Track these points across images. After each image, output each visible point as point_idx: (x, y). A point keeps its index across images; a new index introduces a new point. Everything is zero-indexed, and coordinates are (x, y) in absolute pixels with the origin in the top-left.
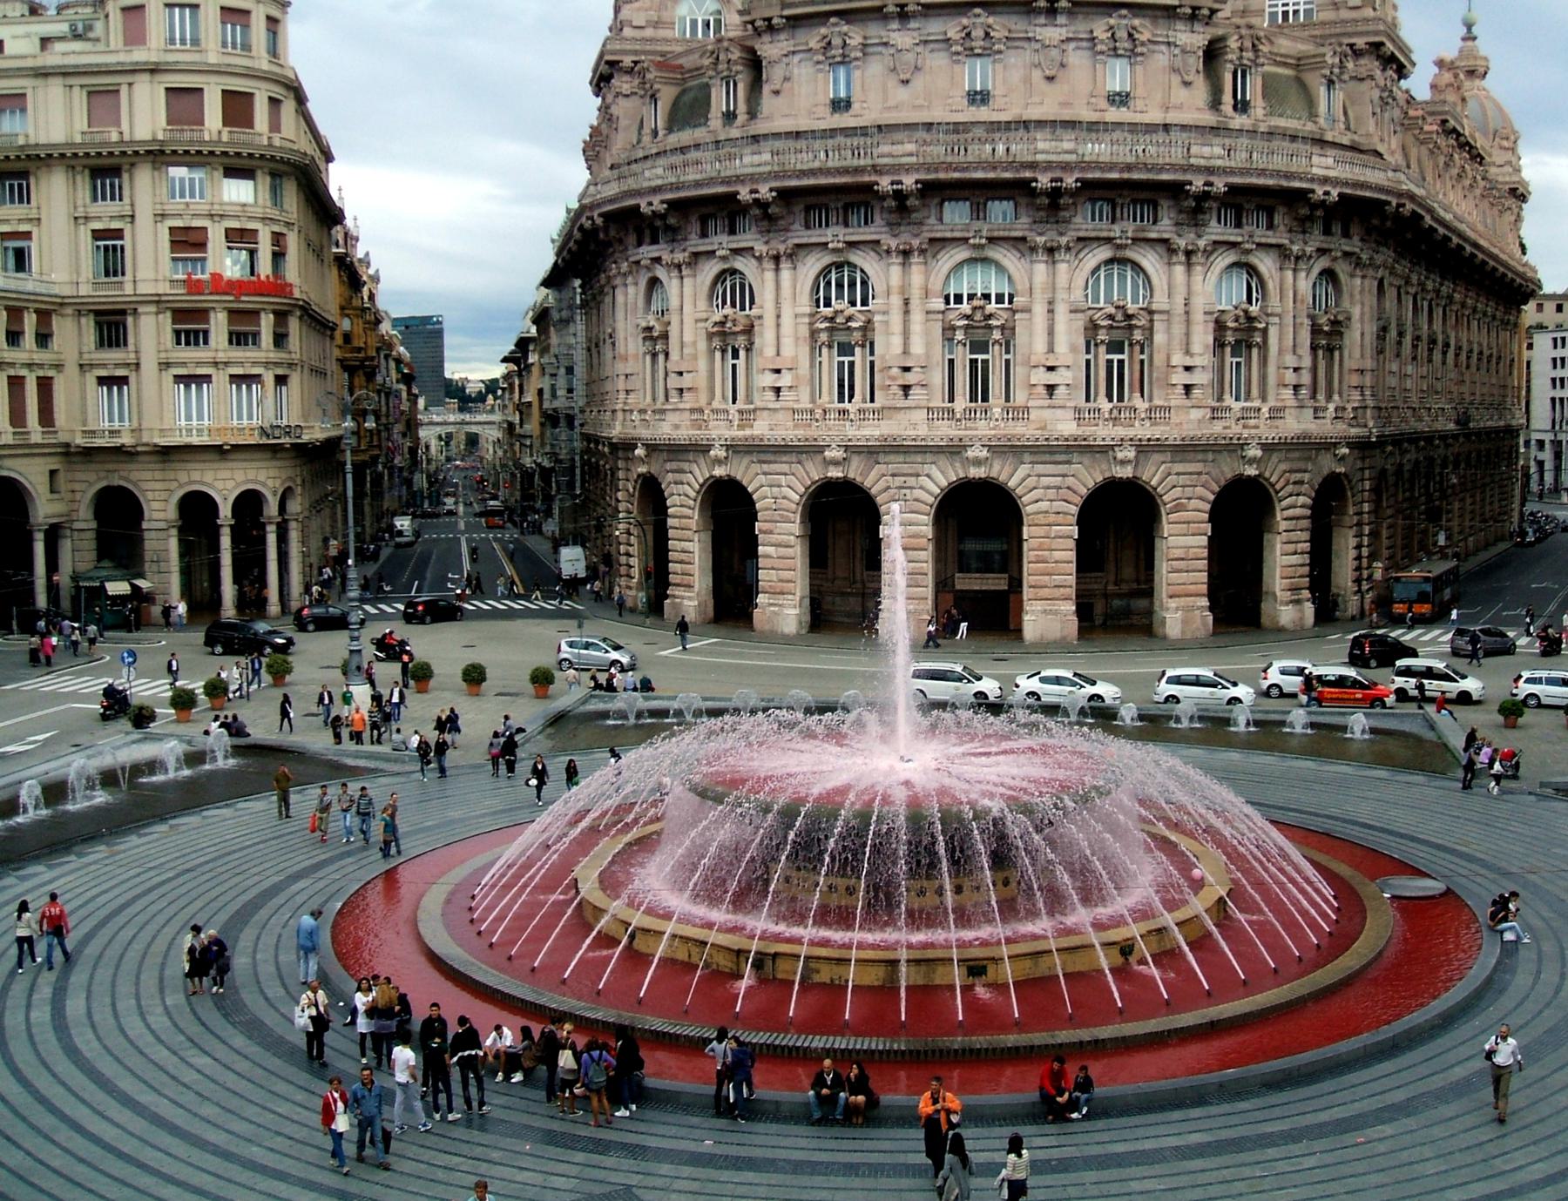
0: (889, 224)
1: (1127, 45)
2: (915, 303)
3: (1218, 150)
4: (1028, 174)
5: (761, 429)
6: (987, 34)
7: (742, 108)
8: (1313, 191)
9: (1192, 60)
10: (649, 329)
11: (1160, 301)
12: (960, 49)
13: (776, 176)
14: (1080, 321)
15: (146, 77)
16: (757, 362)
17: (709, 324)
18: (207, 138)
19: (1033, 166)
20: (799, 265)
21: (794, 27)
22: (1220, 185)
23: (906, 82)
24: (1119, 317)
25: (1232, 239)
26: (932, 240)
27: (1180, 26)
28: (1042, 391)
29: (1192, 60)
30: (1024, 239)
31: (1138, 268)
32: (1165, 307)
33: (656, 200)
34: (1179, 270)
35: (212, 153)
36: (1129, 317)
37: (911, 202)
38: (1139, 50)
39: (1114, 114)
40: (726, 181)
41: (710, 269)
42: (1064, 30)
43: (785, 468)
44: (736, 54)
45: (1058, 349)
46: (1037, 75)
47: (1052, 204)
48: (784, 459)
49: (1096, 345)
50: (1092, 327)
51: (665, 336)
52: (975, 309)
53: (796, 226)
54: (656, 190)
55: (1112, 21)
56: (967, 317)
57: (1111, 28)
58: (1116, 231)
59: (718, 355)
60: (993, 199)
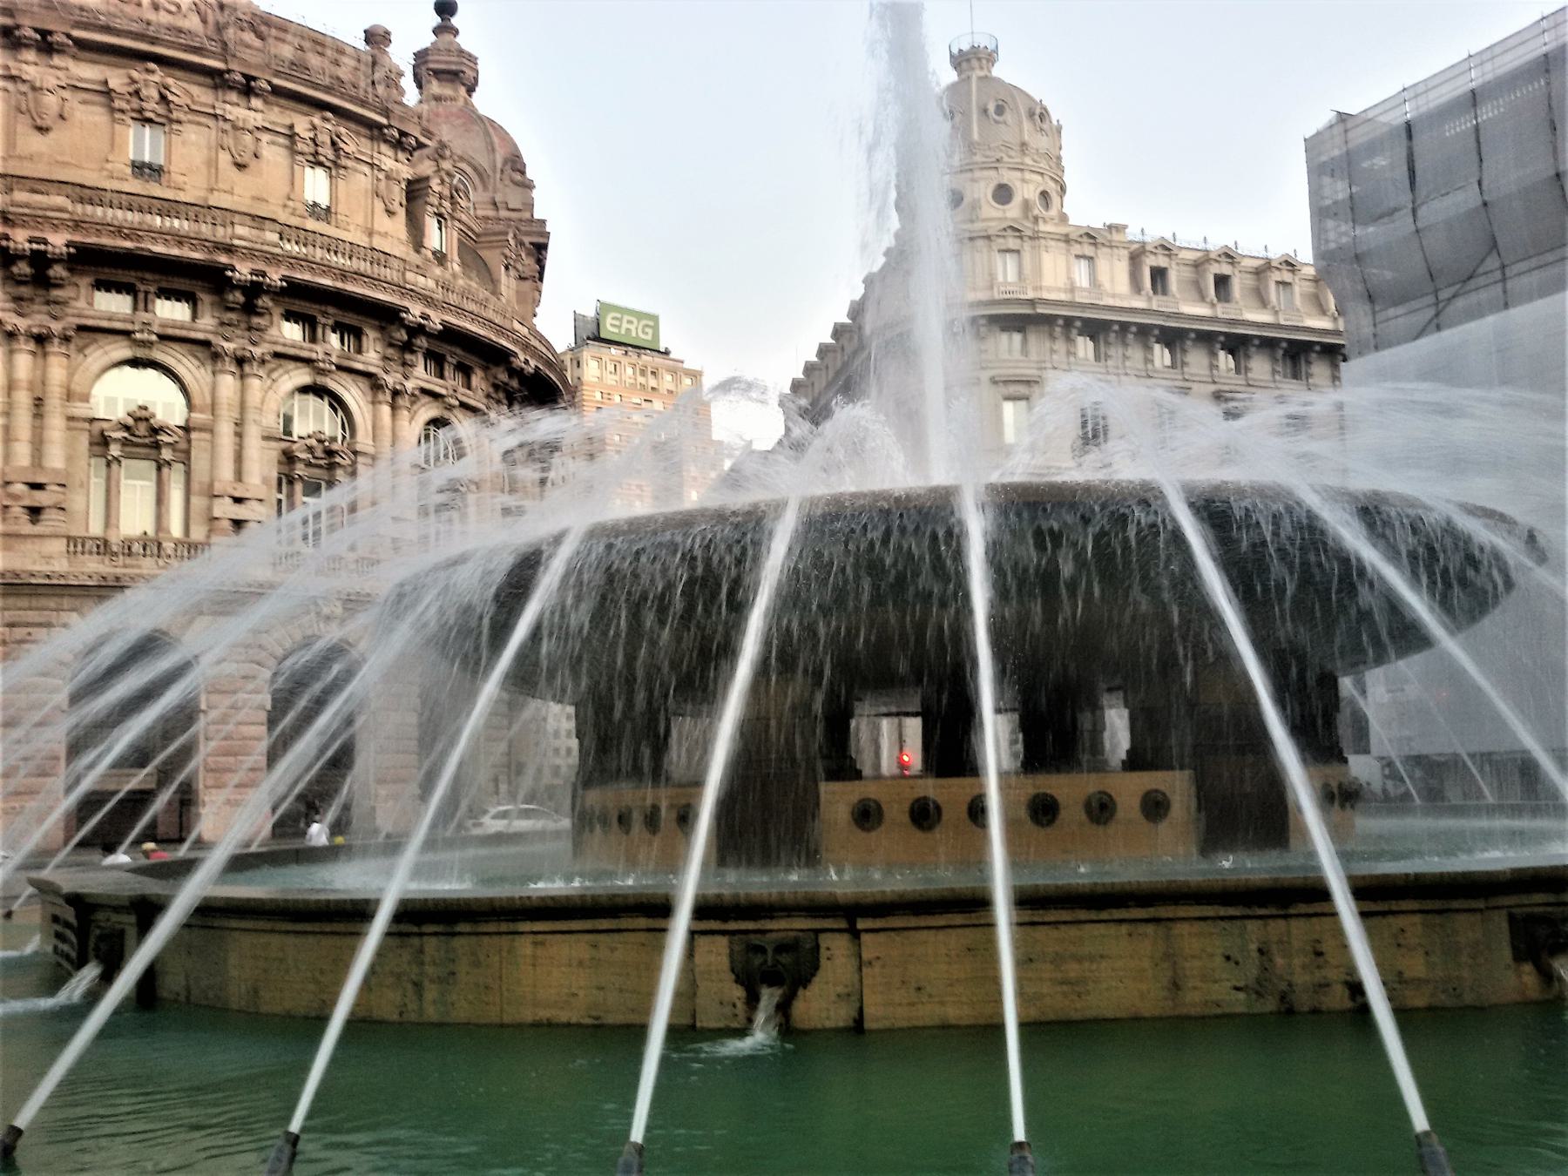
0: (18, 299)
1: (330, 153)
2: (54, 402)
3: (431, 284)
4: (223, 259)
6: (163, 98)
8: (515, 355)
9: (396, 189)
11: (364, 441)
12: (124, 106)
14: (274, 451)
19: (229, 249)
22: (436, 320)
23: (42, 130)
24: (319, 453)
25: (438, 389)
26: (81, 329)
27: (384, 148)
28: (226, 524)
29: (396, 189)
30: (206, 344)
31: (337, 403)
32: (371, 450)
34: (386, 410)
36: (330, 453)
37: (58, 271)
38: (344, 162)
39: (311, 224)
42: (259, 116)
45: (245, 478)
46: (224, 158)
47: (250, 301)
49: (291, 482)
50: (289, 458)
52: (137, 420)
55: (317, 121)
56: (127, 428)
57: (314, 128)
58: (317, 351)
60: (168, 294)
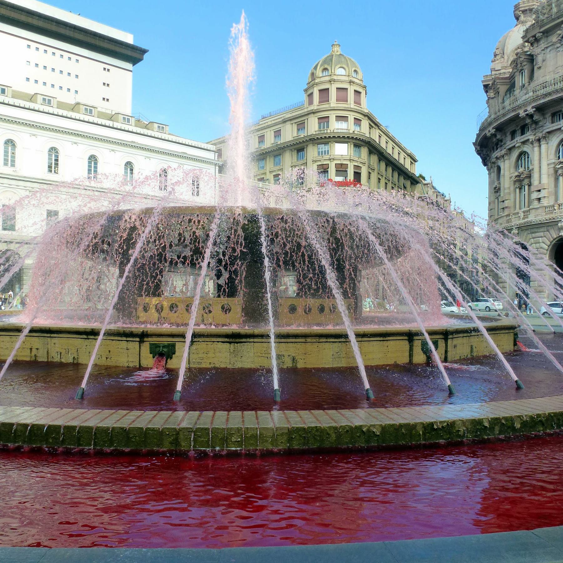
5: (532, 218)
7: (527, 80)
10: (495, 188)
13: (534, 100)
15: (312, 115)
16: (533, 188)
17: (513, 178)
18: (329, 131)
20: (550, 142)
21: (547, 37)
33: (490, 129)
35: (329, 137)
40: (514, 110)
41: (515, 154)
43: (542, 234)
44: (523, 57)
48: (542, 230)
51: (499, 189)
53: (547, 124)
54: (490, 124)
59: (518, 190)
